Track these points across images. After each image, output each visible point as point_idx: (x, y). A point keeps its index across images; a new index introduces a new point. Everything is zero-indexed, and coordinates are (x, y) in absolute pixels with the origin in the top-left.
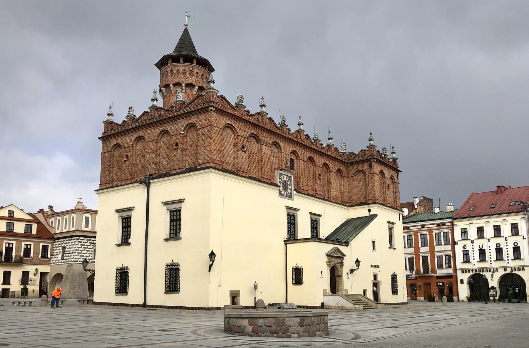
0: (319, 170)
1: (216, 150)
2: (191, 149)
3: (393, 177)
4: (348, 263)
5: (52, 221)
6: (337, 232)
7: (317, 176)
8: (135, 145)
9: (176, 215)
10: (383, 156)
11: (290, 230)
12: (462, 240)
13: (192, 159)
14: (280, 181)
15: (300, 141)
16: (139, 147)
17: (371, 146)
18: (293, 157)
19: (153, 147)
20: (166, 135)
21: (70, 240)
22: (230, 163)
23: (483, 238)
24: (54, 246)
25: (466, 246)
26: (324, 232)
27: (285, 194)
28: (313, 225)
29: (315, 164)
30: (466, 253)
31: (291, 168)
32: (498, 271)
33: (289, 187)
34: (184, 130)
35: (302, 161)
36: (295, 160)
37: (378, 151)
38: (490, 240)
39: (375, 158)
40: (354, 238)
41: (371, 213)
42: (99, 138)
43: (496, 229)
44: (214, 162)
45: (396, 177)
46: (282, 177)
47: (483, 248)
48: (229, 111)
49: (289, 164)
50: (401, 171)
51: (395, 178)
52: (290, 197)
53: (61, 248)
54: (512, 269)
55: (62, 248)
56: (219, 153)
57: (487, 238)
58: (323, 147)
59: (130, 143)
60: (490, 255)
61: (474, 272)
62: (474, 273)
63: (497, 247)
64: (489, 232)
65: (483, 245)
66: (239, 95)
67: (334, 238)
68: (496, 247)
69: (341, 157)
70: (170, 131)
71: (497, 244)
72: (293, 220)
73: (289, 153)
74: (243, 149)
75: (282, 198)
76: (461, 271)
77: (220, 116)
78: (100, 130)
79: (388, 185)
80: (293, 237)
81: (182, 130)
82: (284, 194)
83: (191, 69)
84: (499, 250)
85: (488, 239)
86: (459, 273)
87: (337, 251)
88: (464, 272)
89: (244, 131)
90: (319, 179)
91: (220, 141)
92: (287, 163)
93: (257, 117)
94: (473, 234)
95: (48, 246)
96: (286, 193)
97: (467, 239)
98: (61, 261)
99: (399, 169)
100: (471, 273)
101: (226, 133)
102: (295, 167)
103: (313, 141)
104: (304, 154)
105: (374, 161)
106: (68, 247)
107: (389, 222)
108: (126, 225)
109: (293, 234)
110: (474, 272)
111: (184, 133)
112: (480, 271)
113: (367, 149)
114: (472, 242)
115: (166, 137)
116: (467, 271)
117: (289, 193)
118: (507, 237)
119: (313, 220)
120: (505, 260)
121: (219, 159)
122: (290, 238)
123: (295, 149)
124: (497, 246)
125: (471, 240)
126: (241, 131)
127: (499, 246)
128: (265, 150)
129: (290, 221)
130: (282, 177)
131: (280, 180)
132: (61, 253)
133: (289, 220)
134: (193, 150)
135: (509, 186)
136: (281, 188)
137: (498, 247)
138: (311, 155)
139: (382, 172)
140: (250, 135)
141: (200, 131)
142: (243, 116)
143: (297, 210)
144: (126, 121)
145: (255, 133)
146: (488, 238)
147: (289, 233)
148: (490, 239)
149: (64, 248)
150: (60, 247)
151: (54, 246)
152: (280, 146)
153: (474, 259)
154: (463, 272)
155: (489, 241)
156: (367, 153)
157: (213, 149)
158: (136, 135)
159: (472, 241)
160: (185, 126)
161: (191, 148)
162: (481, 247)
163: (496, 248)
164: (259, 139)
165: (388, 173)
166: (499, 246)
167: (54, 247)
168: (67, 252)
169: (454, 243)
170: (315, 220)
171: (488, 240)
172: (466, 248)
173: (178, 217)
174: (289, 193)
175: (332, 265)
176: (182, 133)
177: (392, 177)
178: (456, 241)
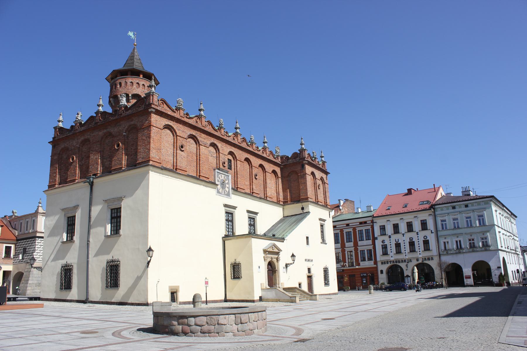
0: (256, 171)
1: (155, 149)
2: (132, 149)
3: (323, 178)
4: (284, 258)
5: (15, 224)
6: (273, 229)
7: (254, 176)
8: (81, 147)
9: (117, 213)
10: (314, 159)
11: (228, 227)
12: (381, 235)
13: (132, 159)
14: (218, 179)
15: (237, 143)
16: (85, 150)
17: (302, 149)
18: (230, 157)
19: (97, 149)
20: (110, 137)
21: (31, 241)
22: (169, 162)
24: (17, 247)
25: (384, 241)
26: (261, 229)
27: (223, 192)
28: (251, 223)
29: (251, 164)
30: (385, 247)
31: (229, 168)
33: (227, 186)
34: (126, 131)
35: (239, 161)
36: (233, 161)
37: (309, 154)
38: (404, 235)
39: (306, 160)
40: (289, 234)
41: (305, 211)
42: (49, 143)
43: (409, 225)
44: (153, 160)
45: (326, 178)
46: (220, 176)
47: (399, 242)
48: (169, 113)
49: (227, 163)
50: (330, 173)
51: (325, 179)
52: (228, 195)
53: (22, 248)
55: (23, 248)
56: (158, 152)
57: (401, 233)
58: (258, 150)
59: (77, 146)
61: (392, 263)
62: (392, 264)
63: (410, 241)
64: (403, 228)
65: (398, 239)
66: (179, 99)
67: (271, 234)
68: (409, 241)
69: (276, 159)
70: (113, 133)
71: (410, 238)
72: (231, 218)
73: (227, 154)
74: (182, 148)
75: (220, 196)
76: (381, 263)
77: (160, 117)
78: (51, 135)
79: (319, 186)
80: (231, 234)
81: (124, 131)
82: (222, 192)
83: (138, 81)
84: (412, 244)
86: (379, 264)
87: (274, 246)
88: (384, 263)
89: (183, 131)
90: (256, 179)
91: (159, 139)
92: (224, 163)
93: (196, 120)
94: (389, 230)
95: (11, 247)
96: (224, 191)
97: (385, 235)
98: (22, 260)
99: (327, 171)
100: (389, 265)
101: (165, 134)
102: (233, 167)
103: (249, 143)
104: (241, 155)
105: (306, 163)
106: (29, 247)
107: (320, 219)
108: (71, 223)
109: (231, 231)
110: (392, 263)
111: (125, 134)
112: (396, 262)
113: (299, 152)
114: (390, 237)
115: (109, 138)
116: (386, 263)
117: (227, 192)
119: (250, 218)
121: (158, 158)
122: (229, 234)
123: (232, 151)
124: (410, 240)
125: (389, 235)
126: (180, 132)
127: (412, 240)
128: (204, 150)
129: (228, 219)
130: (220, 176)
131: (218, 179)
132: (22, 253)
133: (227, 217)
134: (134, 149)
135: (417, 189)
136: (219, 187)
137: (411, 241)
138: (248, 157)
139: (313, 174)
140: (189, 136)
141: (140, 131)
142: (182, 118)
143: (235, 208)
144: (74, 126)
145: (194, 134)
146: (402, 233)
147: (227, 230)
148: (404, 234)
149: (25, 249)
150: (22, 247)
151: (17, 247)
152: (217, 147)
153: (391, 252)
154: (382, 263)
155: (403, 236)
156: (299, 156)
157: (152, 148)
158: (83, 138)
159: (389, 236)
160: (127, 127)
161: (132, 148)
162: (397, 241)
163: (409, 242)
164: (198, 140)
165: (318, 174)
166: (412, 240)
167: (17, 248)
168: (27, 252)
169: (374, 239)
170: (252, 218)
171: (402, 235)
172: (385, 242)
173: (119, 215)
174: (227, 192)
175: (269, 260)
176: (124, 134)
177: (322, 179)
178: (376, 236)
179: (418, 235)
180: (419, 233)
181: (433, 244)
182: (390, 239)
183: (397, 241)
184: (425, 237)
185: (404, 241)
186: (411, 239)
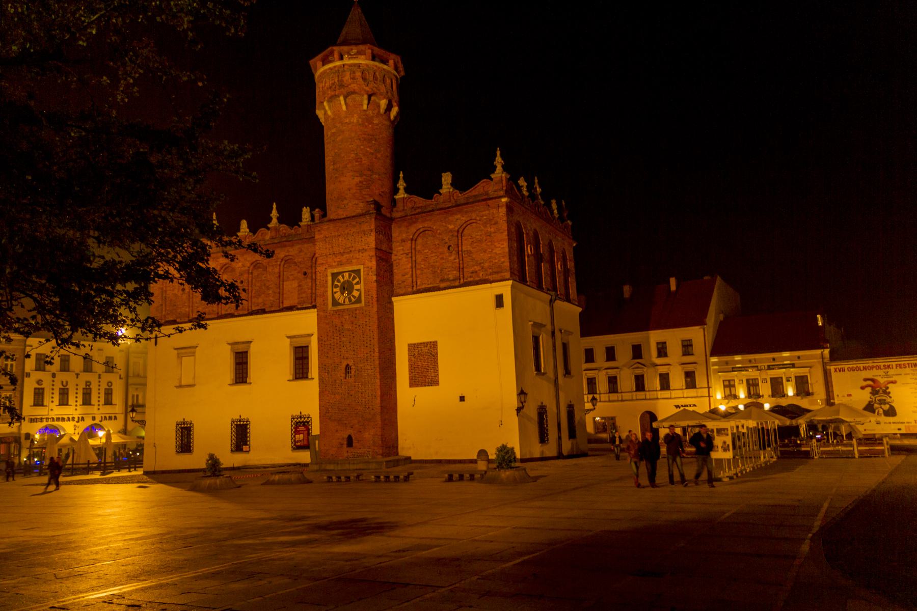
23: (68, 371)
25: (42, 381)
32: (84, 421)
38: (79, 376)
47: (67, 387)
54: (102, 417)
60: (99, 397)
63: (86, 386)
65: (67, 382)
68: (84, 387)
85: (76, 374)
118: (100, 373)
120: (94, 405)
124: (86, 385)
137: (88, 387)
155: (77, 378)
162: (64, 383)
166: (89, 386)
171: (75, 376)
172: (42, 384)
178: (27, 370)
179: (100, 380)
180: (102, 376)
181: (118, 398)
182: (55, 379)
183: (64, 383)
184: (39, 382)
185: (77, 385)
186: (88, 384)
